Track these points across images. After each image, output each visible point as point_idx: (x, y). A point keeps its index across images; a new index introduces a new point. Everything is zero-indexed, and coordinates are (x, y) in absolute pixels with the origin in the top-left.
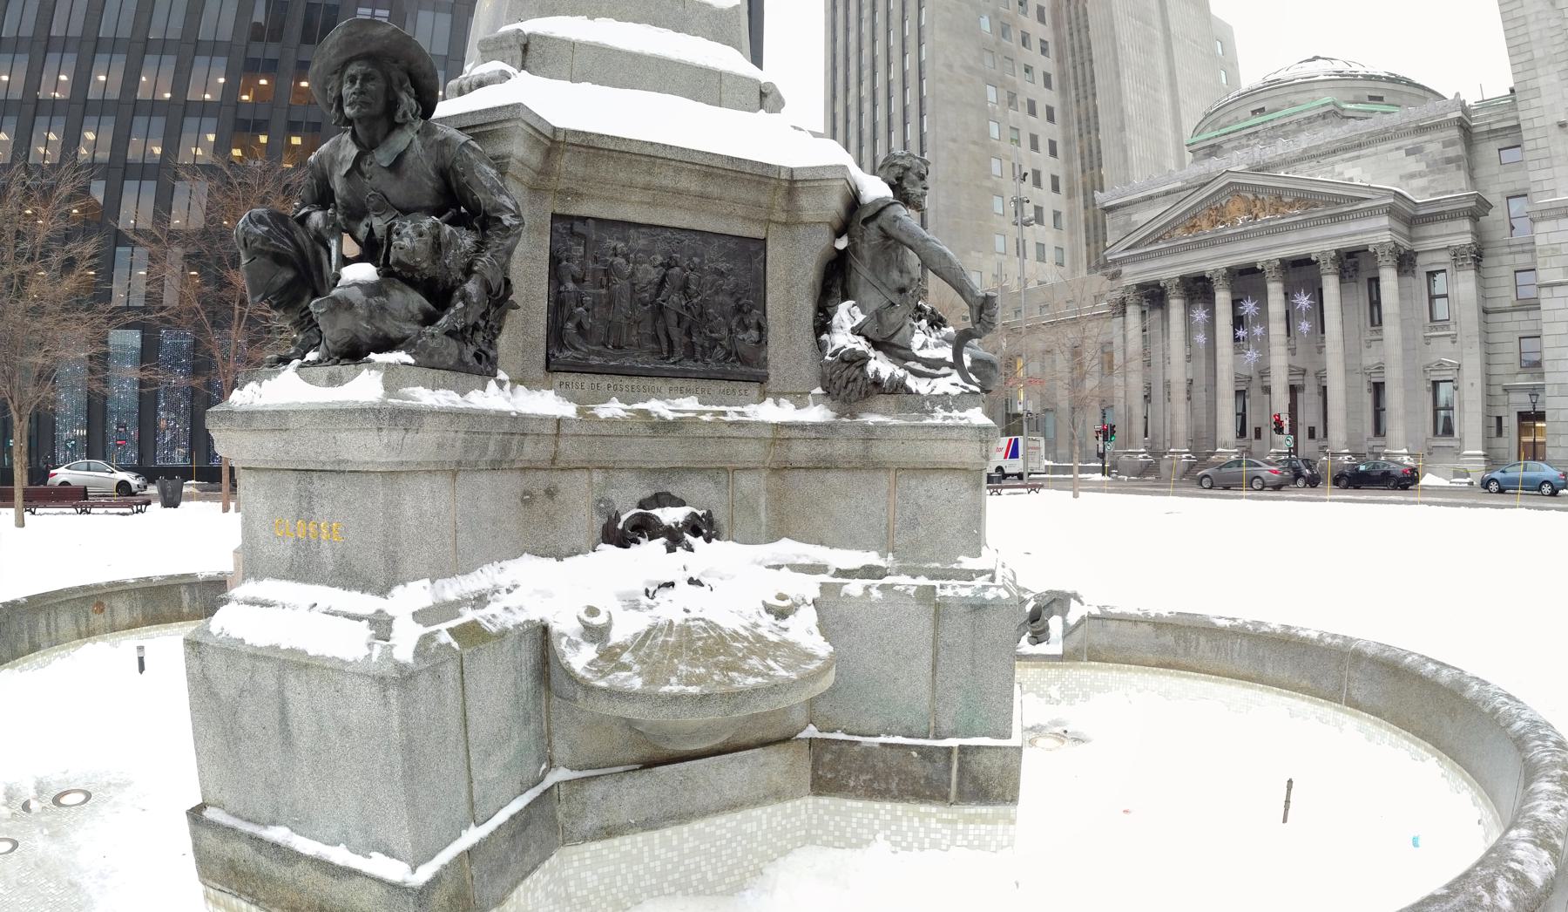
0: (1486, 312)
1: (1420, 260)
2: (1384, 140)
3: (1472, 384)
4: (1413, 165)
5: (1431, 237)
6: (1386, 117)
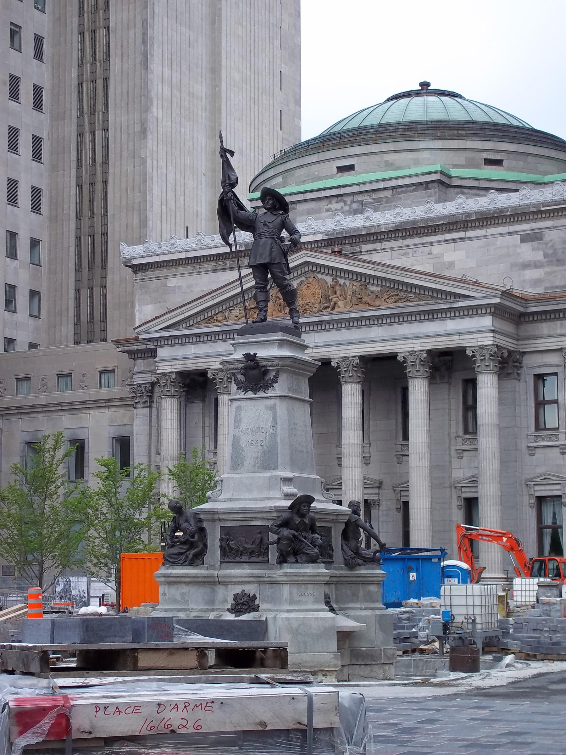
1: (528, 361)
5: (542, 337)
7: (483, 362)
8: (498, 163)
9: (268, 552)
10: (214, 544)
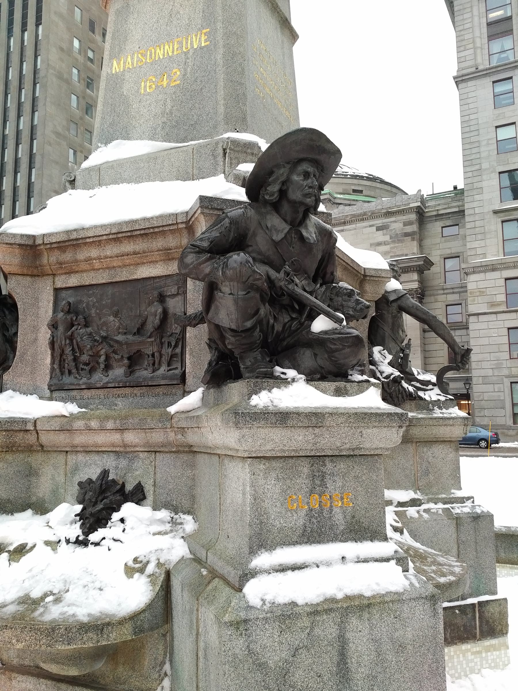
2: (363, 220)
6: (366, 205)
8: (361, 192)
9: (183, 353)
10: (36, 339)
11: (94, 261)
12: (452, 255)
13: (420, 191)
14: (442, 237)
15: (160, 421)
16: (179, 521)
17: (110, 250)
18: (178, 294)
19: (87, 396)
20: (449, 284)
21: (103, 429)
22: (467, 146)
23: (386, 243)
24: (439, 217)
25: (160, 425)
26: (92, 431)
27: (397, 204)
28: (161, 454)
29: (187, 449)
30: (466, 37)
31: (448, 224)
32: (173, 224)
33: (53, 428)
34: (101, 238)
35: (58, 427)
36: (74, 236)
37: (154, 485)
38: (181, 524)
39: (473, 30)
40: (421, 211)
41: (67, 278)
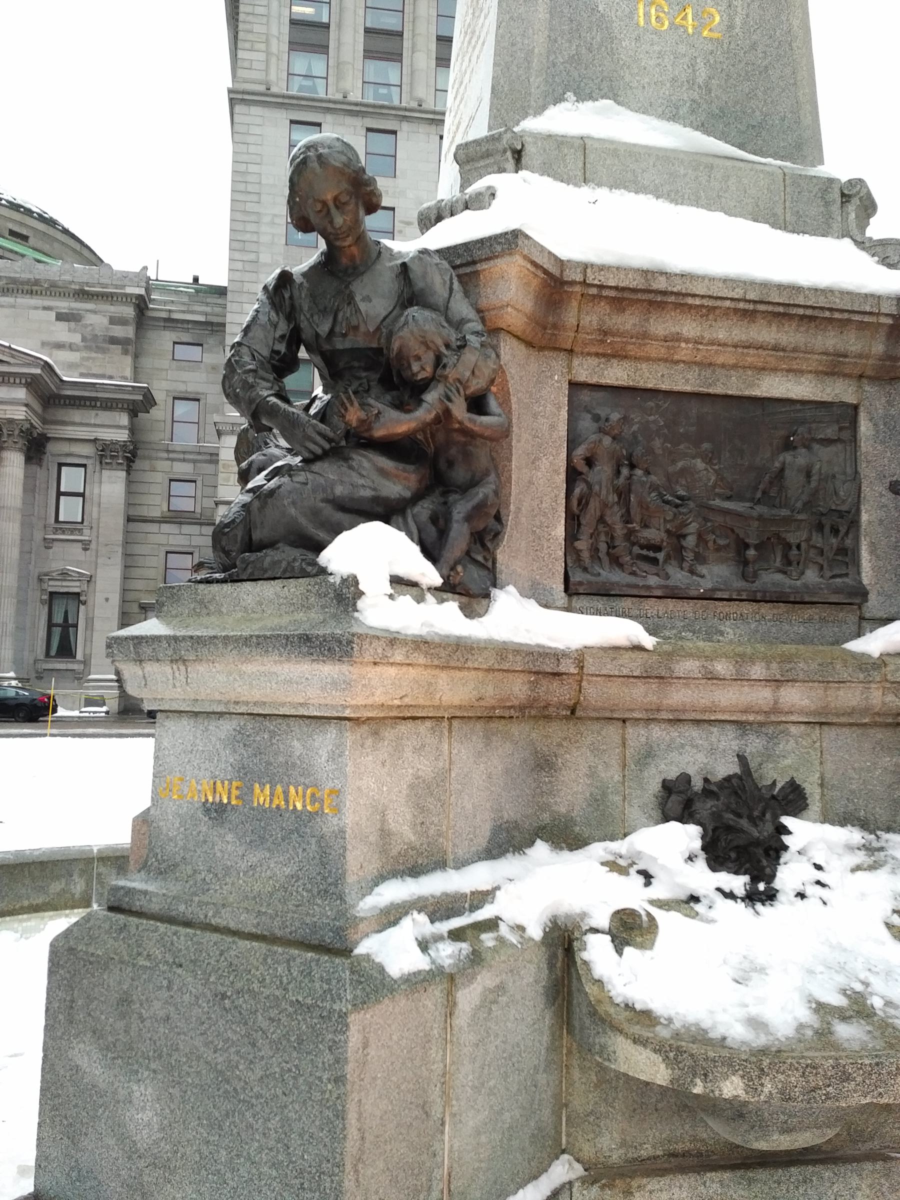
0: (129, 519)
1: (51, 447)
3: (107, 600)
4: (62, 332)
5: (74, 424)
6: (40, 266)
7: (11, 438)
8: (25, 238)
11: (683, 345)
12: (187, 395)
13: (145, 268)
14: (173, 359)
15: (861, 669)
16: (875, 844)
17: (725, 330)
18: (839, 440)
19: (655, 612)
20: (177, 444)
21: (740, 679)
22: (239, 216)
23: (74, 347)
24: (170, 323)
25: (861, 676)
26: (715, 681)
27: (102, 281)
28: (833, 728)
29: (890, 720)
30: (257, 28)
31: (184, 340)
32: (870, 313)
33: (625, 672)
34: (719, 303)
35: (638, 671)
36: (661, 284)
37: (822, 785)
38: (882, 849)
39: (268, 21)
40: (143, 306)
41: (602, 366)
